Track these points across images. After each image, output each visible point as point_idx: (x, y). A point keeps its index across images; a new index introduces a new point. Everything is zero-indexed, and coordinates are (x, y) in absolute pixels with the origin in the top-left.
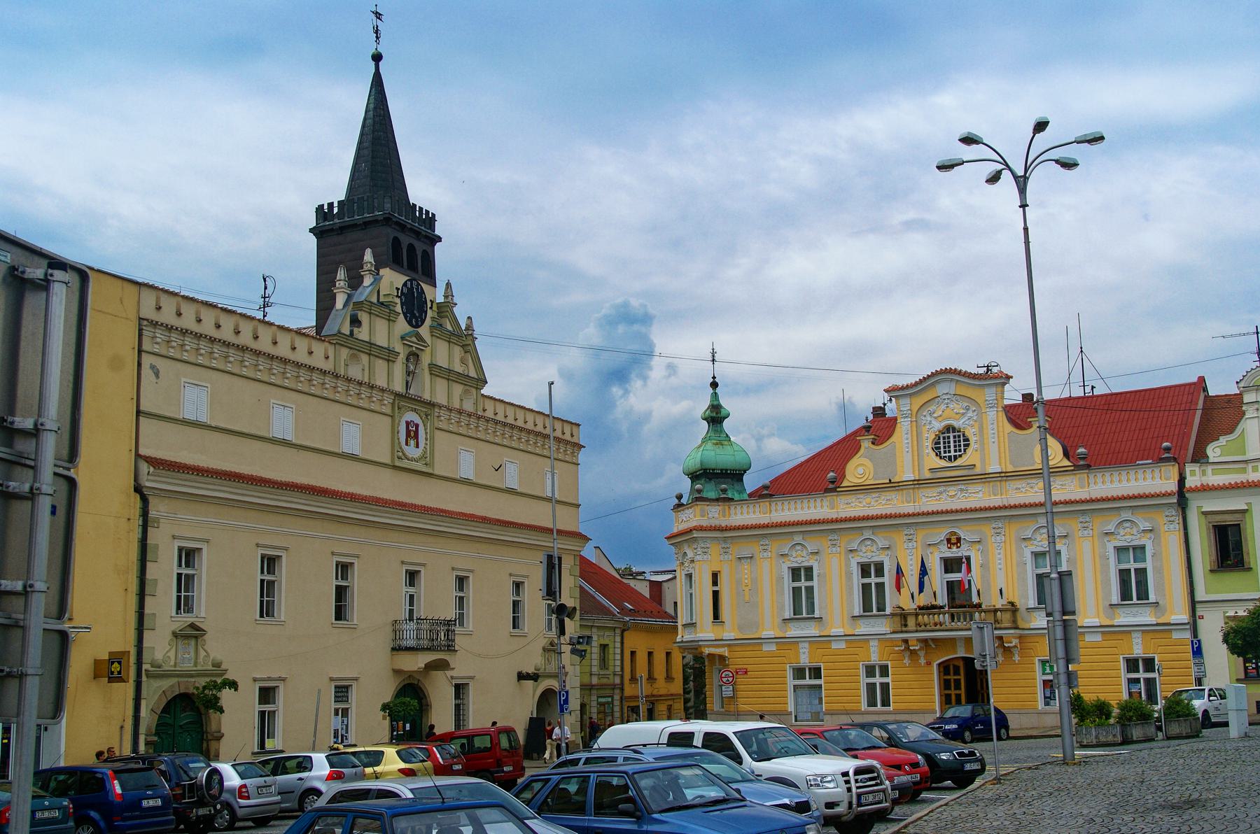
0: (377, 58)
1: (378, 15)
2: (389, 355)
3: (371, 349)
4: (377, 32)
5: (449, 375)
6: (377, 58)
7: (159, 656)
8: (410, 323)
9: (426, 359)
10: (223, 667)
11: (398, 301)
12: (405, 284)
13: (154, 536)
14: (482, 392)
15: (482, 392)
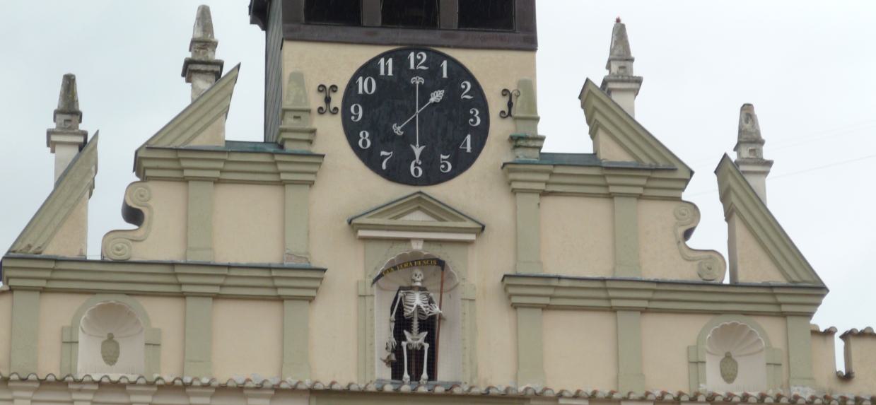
8: (396, 174)
12: (369, 69)
14: (821, 319)
15: (821, 319)
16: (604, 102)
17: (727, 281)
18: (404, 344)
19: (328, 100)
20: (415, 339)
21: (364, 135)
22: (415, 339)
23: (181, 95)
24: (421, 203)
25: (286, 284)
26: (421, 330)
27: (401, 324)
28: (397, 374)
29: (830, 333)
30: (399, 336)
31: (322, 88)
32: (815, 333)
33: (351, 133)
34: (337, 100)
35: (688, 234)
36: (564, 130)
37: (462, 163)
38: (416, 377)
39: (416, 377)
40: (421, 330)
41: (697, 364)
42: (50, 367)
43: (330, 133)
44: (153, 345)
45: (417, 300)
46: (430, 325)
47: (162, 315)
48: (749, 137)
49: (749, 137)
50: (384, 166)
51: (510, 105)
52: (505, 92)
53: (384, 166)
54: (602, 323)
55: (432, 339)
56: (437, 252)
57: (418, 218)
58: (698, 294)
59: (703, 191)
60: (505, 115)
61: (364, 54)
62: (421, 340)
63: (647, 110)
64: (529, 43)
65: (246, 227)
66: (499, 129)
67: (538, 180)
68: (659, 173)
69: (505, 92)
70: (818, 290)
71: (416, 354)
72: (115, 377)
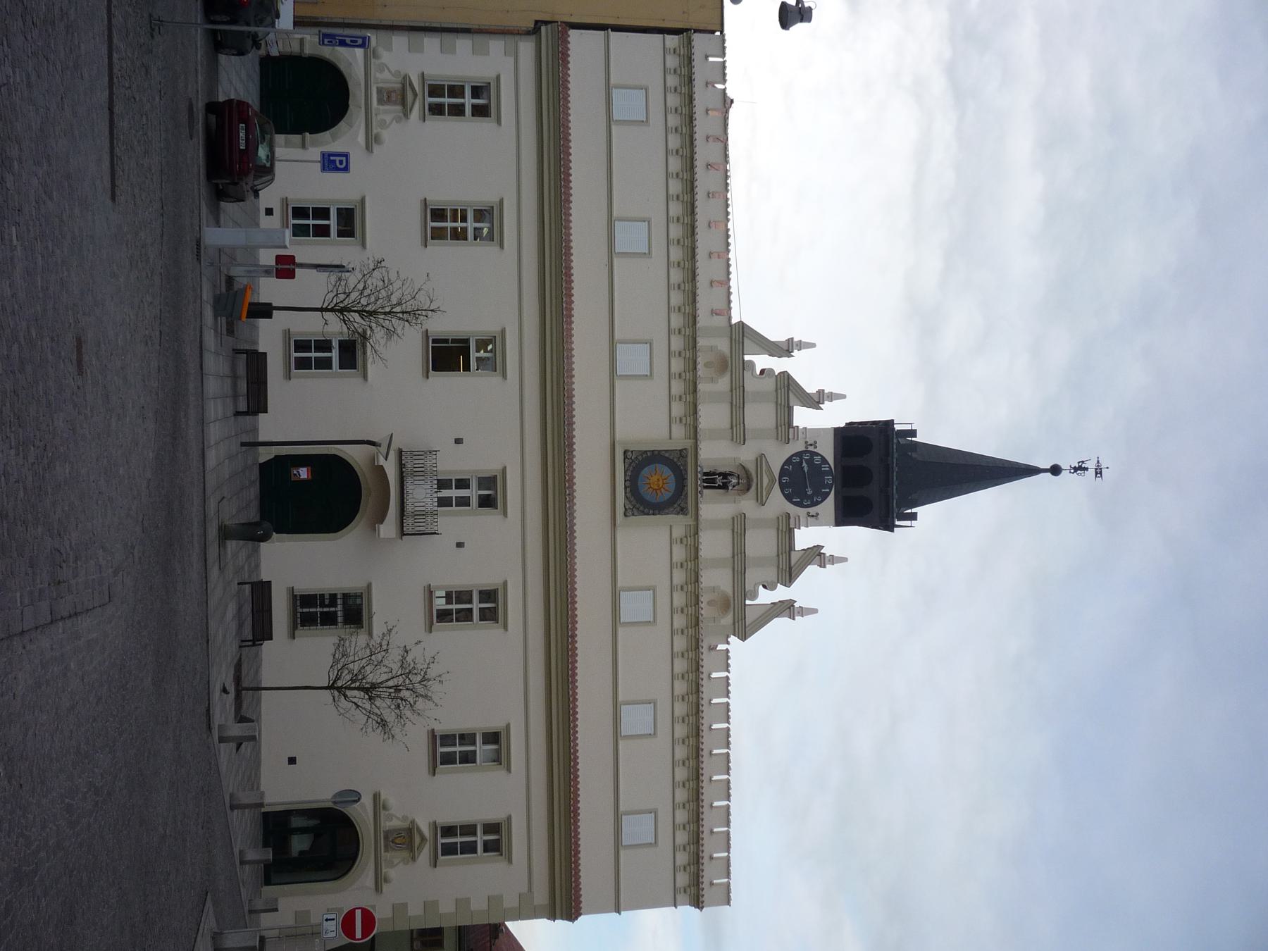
0: (1055, 470)
1: (1098, 472)
2: (738, 432)
3: (737, 399)
4: (1080, 468)
5: (739, 563)
6: (1055, 470)
7: (385, 57)
8: (783, 472)
9: (747, 504)
10: (376, 148)
11: (800, 447)
12: (824, 461)
13: (496, 46)
14: (733, 639)
16: (816, 555)
17: (748, 602)
21: (798, 459)
22: (719, 481)
23: (811, 389)
24: (772, 481)
25: (738, 432)
27: (725, 475)
28: (705, 474)
29: (728, 643)
30: (720, 474)
32: (728, 637)
33: (800, 454)
34: (811, 448)
35: (764, 587)
36: (804, 537)
37: (789, 498)
38: (704, 481)
39: (704, 481)
41: (714, 589)
42: (701, 342)
43: (799, 446)
44: (712, 380)
45: (734, 481)
46: (724, 487)
47: (723, 384)
48: (803, 612)
49: (803, 612)
54: (728, 554)
55: (719, 487)
56: (753, 488)
57: (766, 481)
58: (743, 592)
59: (781, 593)
60: (809, 515)
61: (831, 460)
63: (812, 570)
64: (839, 523)
65: (759, 416)
66: (802, 512)
67: (783, 527)
68: (788, 575)
70: (744, 638)
71: (713, 481)
72: (699, 367)
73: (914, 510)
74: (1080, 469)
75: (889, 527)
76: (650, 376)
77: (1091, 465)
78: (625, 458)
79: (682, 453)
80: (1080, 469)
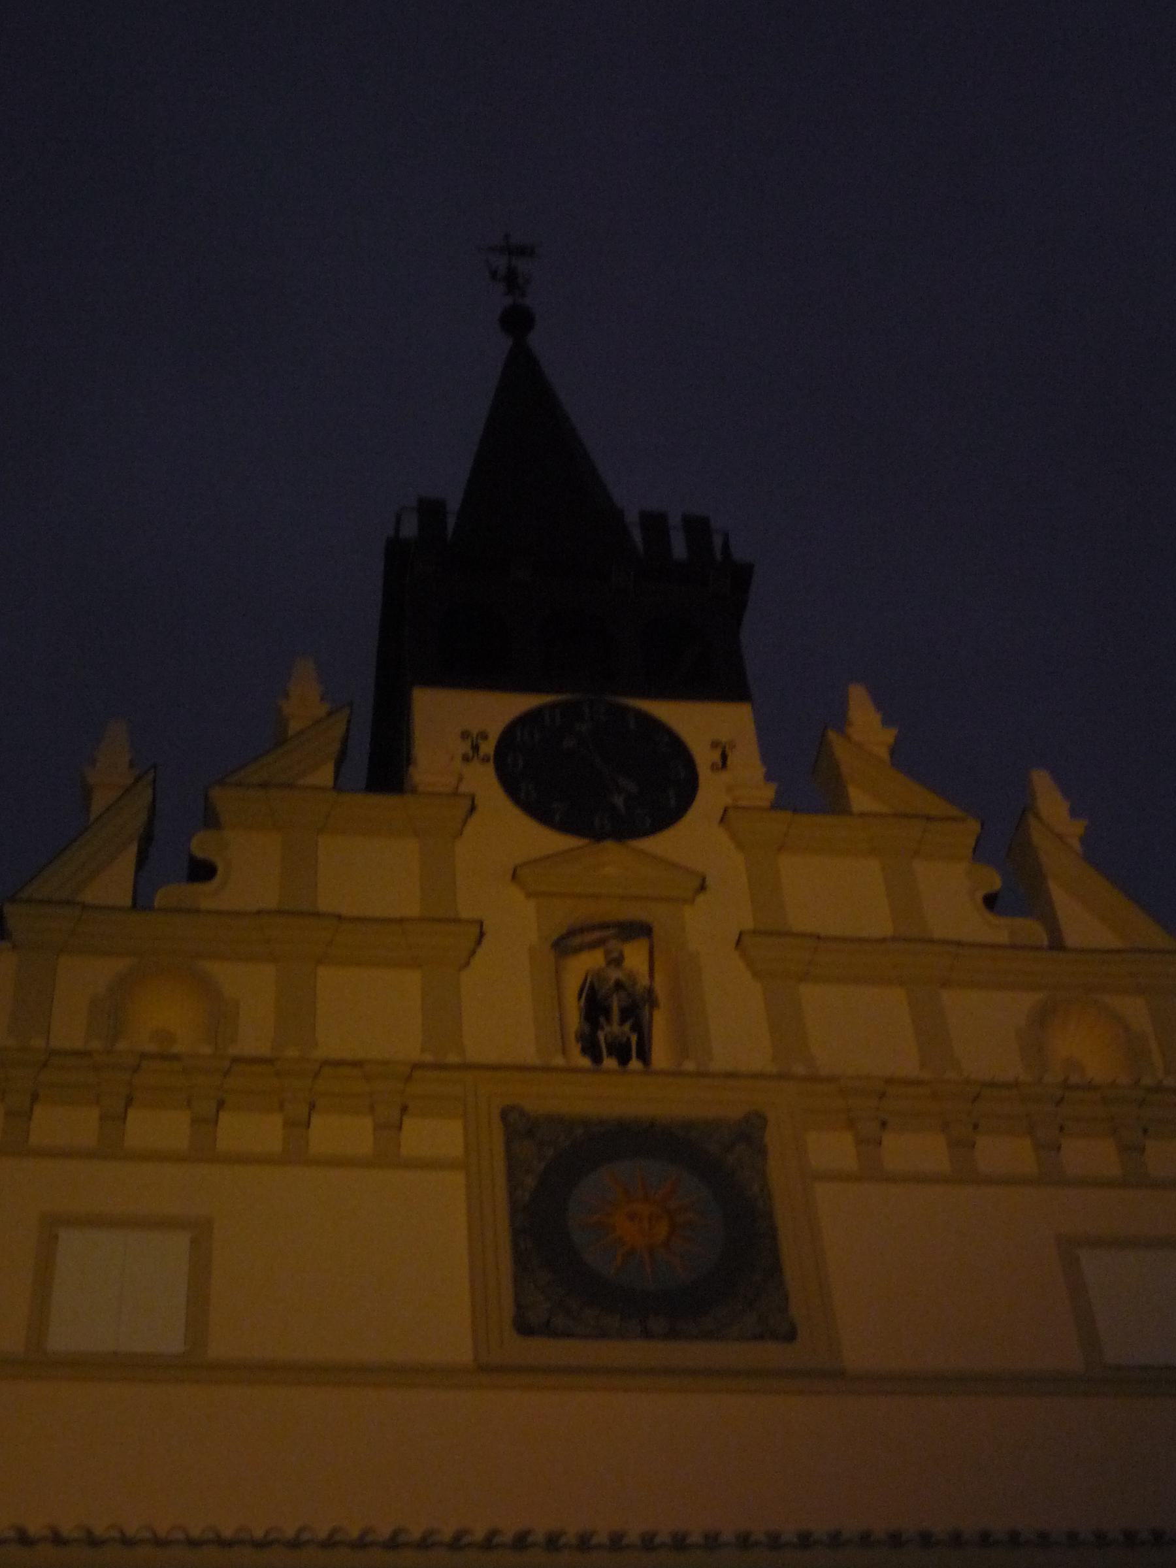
0: (517, 321)
6: (517, 321)
18: (601, 1036)
19: (476, 748)
20: (614, 1028)
26: (622, 1021)
27: (595, 1006)
31: (465, 735)
34: (488, 748)
40: (622, 1021)
46: (637, 1010)
50: (557, 818)
51: (724, 757)
52: (715, 745)
53: (557, 818)
62: (627, 1027)
69: (715, 745)
73: (675, 520)
74: (512, 281)
75: (741, 576)
76: (200, 1232)
77: (501, 262)
78: (547, 1330)
79: (520, 1127)
80: (512, 281)
